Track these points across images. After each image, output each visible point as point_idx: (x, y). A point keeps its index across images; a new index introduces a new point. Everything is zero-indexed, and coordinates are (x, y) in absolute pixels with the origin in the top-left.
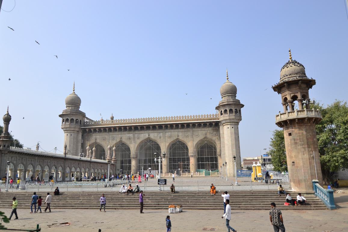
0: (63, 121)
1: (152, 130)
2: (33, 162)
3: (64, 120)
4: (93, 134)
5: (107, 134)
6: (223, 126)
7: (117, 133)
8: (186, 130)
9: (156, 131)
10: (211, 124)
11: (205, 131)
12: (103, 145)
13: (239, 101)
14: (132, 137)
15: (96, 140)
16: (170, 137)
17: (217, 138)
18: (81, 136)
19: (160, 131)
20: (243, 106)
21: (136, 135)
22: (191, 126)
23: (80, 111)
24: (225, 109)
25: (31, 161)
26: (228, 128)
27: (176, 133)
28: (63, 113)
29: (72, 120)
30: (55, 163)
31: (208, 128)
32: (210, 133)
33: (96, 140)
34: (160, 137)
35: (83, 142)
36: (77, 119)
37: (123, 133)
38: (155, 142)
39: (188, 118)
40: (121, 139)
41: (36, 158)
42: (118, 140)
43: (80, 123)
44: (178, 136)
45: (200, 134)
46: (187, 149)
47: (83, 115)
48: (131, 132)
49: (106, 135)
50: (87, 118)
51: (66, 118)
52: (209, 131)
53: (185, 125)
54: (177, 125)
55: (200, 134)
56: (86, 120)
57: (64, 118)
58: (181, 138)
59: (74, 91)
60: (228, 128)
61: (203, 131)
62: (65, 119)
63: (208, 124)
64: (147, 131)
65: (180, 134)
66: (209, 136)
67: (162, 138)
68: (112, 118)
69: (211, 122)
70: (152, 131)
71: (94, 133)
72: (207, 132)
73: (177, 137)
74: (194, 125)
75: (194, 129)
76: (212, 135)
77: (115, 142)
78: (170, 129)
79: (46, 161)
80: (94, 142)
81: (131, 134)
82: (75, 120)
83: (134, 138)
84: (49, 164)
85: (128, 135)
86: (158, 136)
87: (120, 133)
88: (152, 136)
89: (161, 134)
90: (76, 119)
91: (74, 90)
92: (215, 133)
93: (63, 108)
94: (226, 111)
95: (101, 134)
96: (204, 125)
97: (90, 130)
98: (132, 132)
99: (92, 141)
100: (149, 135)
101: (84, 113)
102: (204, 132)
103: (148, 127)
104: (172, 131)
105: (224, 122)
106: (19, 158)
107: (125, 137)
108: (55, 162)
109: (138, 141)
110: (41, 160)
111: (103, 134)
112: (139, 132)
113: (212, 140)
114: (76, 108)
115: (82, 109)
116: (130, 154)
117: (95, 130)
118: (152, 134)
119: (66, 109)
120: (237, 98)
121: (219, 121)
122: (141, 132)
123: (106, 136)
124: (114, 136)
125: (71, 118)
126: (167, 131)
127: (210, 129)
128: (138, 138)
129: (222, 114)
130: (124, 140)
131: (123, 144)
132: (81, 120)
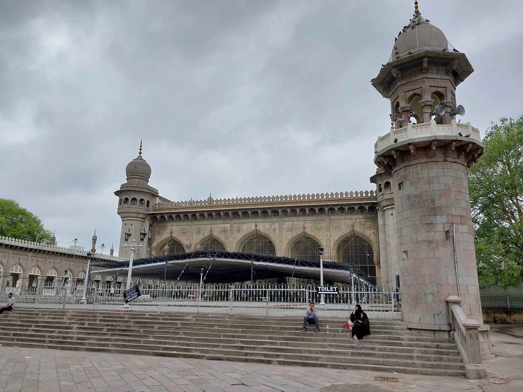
1: (261, 217)
2: (21, 261)
3: (121, 200)
4: (168, 224)
5: (189, 223)
6: (384, 211)
7: (205, 222)
8: (319, 218)
9: (268, 220)
10: (361, 208)
11: (351, 221)
14: (229, 228)
15: (171, 233)
16: (291, 229)
17: (374, 233)
18: (148, 226)
19: (275, 219)
21: (235, 226)
22: (326, 210)
25: (19, 258)
26: (392, 214)
27: (302, 223)
29: (134, 199)
31: (357, 214)
32: (360, 223)
33: (171, 233)
34: (275, 230)
35: (151, 236)
36: (142, 200)
37: (215, 222)
39: (322, 197)
41: (30, 254)
42: (207, 234)
43: (148, 206)
44: (304, 228)
45: (343, 226)
48: (227, 221)
49: (185, 225)
50: (161, 198)
51: (125, 197)
52: (358, 220)
53: (317, 210)
54: (303, 210)
55: (342, 225)
58: (309, 231)
60: (392, 214)
61: (349, 221)
62: (123, 198)
63: (356, 208)
64: (254, 220)
65: (308, 225)
66: (358, 229)
67: (277, 231)
68: (210, 200)
69: (362, 204)
70: (261, 220)
71: (168, 222)
72: (356, 222)
73: (302, 230)
74: (331, 209)
75: (332, 217)
76: (364, 228)
77: (201, 237)
78: (290, 216)
79: (52, 261)
82: (138, 200)
83: (232, 231)
84: (56, 266)
85: (223, 226)
86: (271, 227)
87: (209, 222)
88: (262, 227)
89: (277, 224)
91: (140, 153)
92: (370, 223)
93: (121, 180)
95: (180, 224)
96: (349, 209)
97: (162, 216)
98: (229, 221)
99: (165, 235)
100: (256, 226)
102: (350, 222)
103: (255, 213)
104: (295, 219)
105: (384, 204)
107: (217, 229)
108: (71, 263)
109: (239, 236)
110: (39, 259)
111: (183, 223)
112: (240, 221)
113: (364, 235)
114: (142, 180)
115: (152, 183)
118: (261, 224)
121: (375, 203)
122: (244, 221)
123: (188, 227)
124: (200, 226)
125: (132, 197)
126: (286, 219)
127: (361, 216)
128: (238, 231)
129: (380, 190)
130: (216, 234)
131: (215, 240)
132: (150, 201)
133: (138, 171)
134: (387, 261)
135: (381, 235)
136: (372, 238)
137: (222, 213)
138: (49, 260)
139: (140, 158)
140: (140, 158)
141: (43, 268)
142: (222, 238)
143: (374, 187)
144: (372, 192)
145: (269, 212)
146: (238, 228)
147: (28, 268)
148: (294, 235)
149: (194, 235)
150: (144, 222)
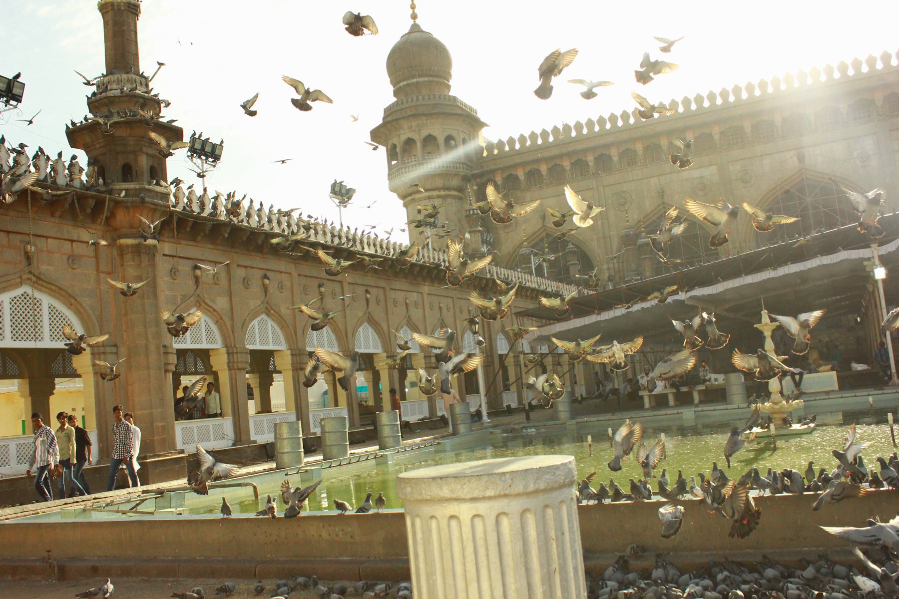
0: (392, 154)
3: (395, 146)
4: (528, 195)
12: (581, 238)
23: (455, 98)
28: (389, 119)
30: (444, 310)
40: (663, 196)
51: (404, 138)
57: (395, 141)
59: (418, 21)
62: (399, 140)
79: (400, 296)
80: (538, 227)
81: (711, 165)
90: (446, 134)
91: (414, 17)
101: (471, 109)
106: (240, 273)
125: (425, 133)
138: (392, 295)
139: (415, 28)
140: (415, 28)
141: (385, 327)
147: (350, 330)
150: (460, 198)
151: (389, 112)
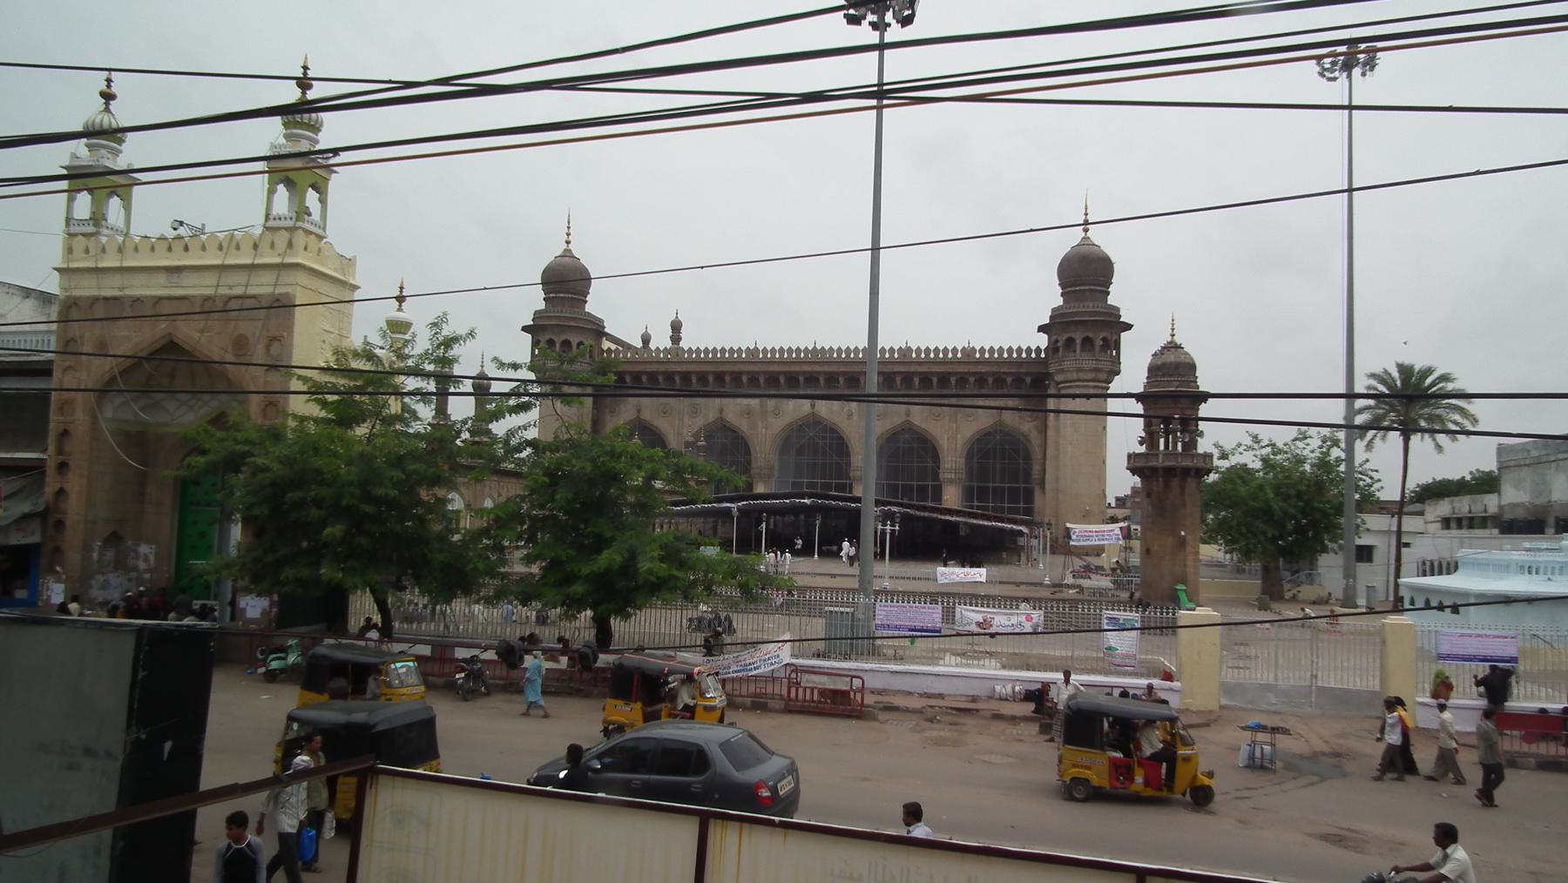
0: (535, 344)
10: (1018, 380)
13: (1118, 309)
20: (1128, 327)
24: (1065, 337)
34: (850, 415)
36: (580, 343)
38: (833, 430)
42: (712, 417)
44: (908, 414)
46: (936, 456)
47: (596, 329)
53: (935, 380)
56: (606, 345)
62: (544, 338)
77: (700, 422)
91: (568, 242)
93: (536, 300)
94: (1070, 341)
96: (995, 381)
100: (813, 406)
107: (734, 409)
109: (778, 424)
115: (593, 306)
116: (749, 463)
117: (637, 377)
119: (542, 305)
120: (1111, 300)
125: (563, 337)
133: (566, 282)
134: (1057, 479)
135: (1050, 433)
136: (1034, 437)
137: (745, 378)
139: (567, 253)
142: (743, 426)
143: (1042, 341)
144: (1038, 350)
145: (841, 380)
146: (776, 407)
148: (888, 426)
149: (686, 419)
151: (538, 315)
